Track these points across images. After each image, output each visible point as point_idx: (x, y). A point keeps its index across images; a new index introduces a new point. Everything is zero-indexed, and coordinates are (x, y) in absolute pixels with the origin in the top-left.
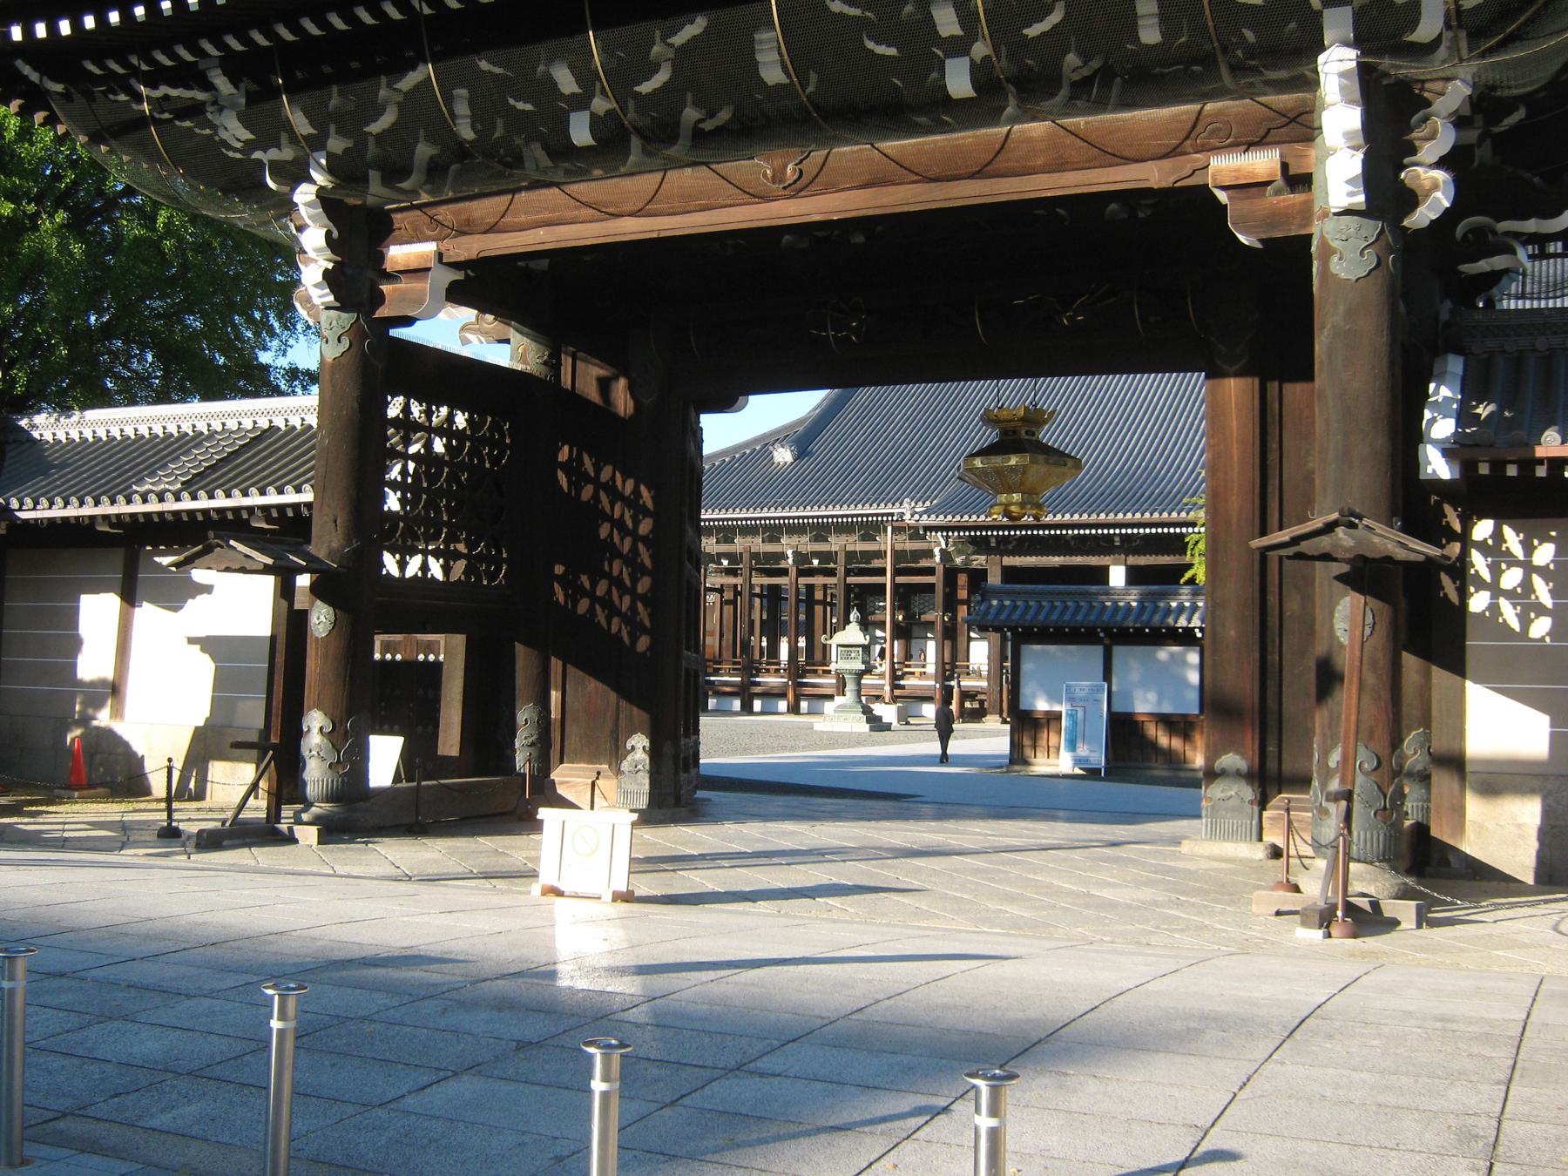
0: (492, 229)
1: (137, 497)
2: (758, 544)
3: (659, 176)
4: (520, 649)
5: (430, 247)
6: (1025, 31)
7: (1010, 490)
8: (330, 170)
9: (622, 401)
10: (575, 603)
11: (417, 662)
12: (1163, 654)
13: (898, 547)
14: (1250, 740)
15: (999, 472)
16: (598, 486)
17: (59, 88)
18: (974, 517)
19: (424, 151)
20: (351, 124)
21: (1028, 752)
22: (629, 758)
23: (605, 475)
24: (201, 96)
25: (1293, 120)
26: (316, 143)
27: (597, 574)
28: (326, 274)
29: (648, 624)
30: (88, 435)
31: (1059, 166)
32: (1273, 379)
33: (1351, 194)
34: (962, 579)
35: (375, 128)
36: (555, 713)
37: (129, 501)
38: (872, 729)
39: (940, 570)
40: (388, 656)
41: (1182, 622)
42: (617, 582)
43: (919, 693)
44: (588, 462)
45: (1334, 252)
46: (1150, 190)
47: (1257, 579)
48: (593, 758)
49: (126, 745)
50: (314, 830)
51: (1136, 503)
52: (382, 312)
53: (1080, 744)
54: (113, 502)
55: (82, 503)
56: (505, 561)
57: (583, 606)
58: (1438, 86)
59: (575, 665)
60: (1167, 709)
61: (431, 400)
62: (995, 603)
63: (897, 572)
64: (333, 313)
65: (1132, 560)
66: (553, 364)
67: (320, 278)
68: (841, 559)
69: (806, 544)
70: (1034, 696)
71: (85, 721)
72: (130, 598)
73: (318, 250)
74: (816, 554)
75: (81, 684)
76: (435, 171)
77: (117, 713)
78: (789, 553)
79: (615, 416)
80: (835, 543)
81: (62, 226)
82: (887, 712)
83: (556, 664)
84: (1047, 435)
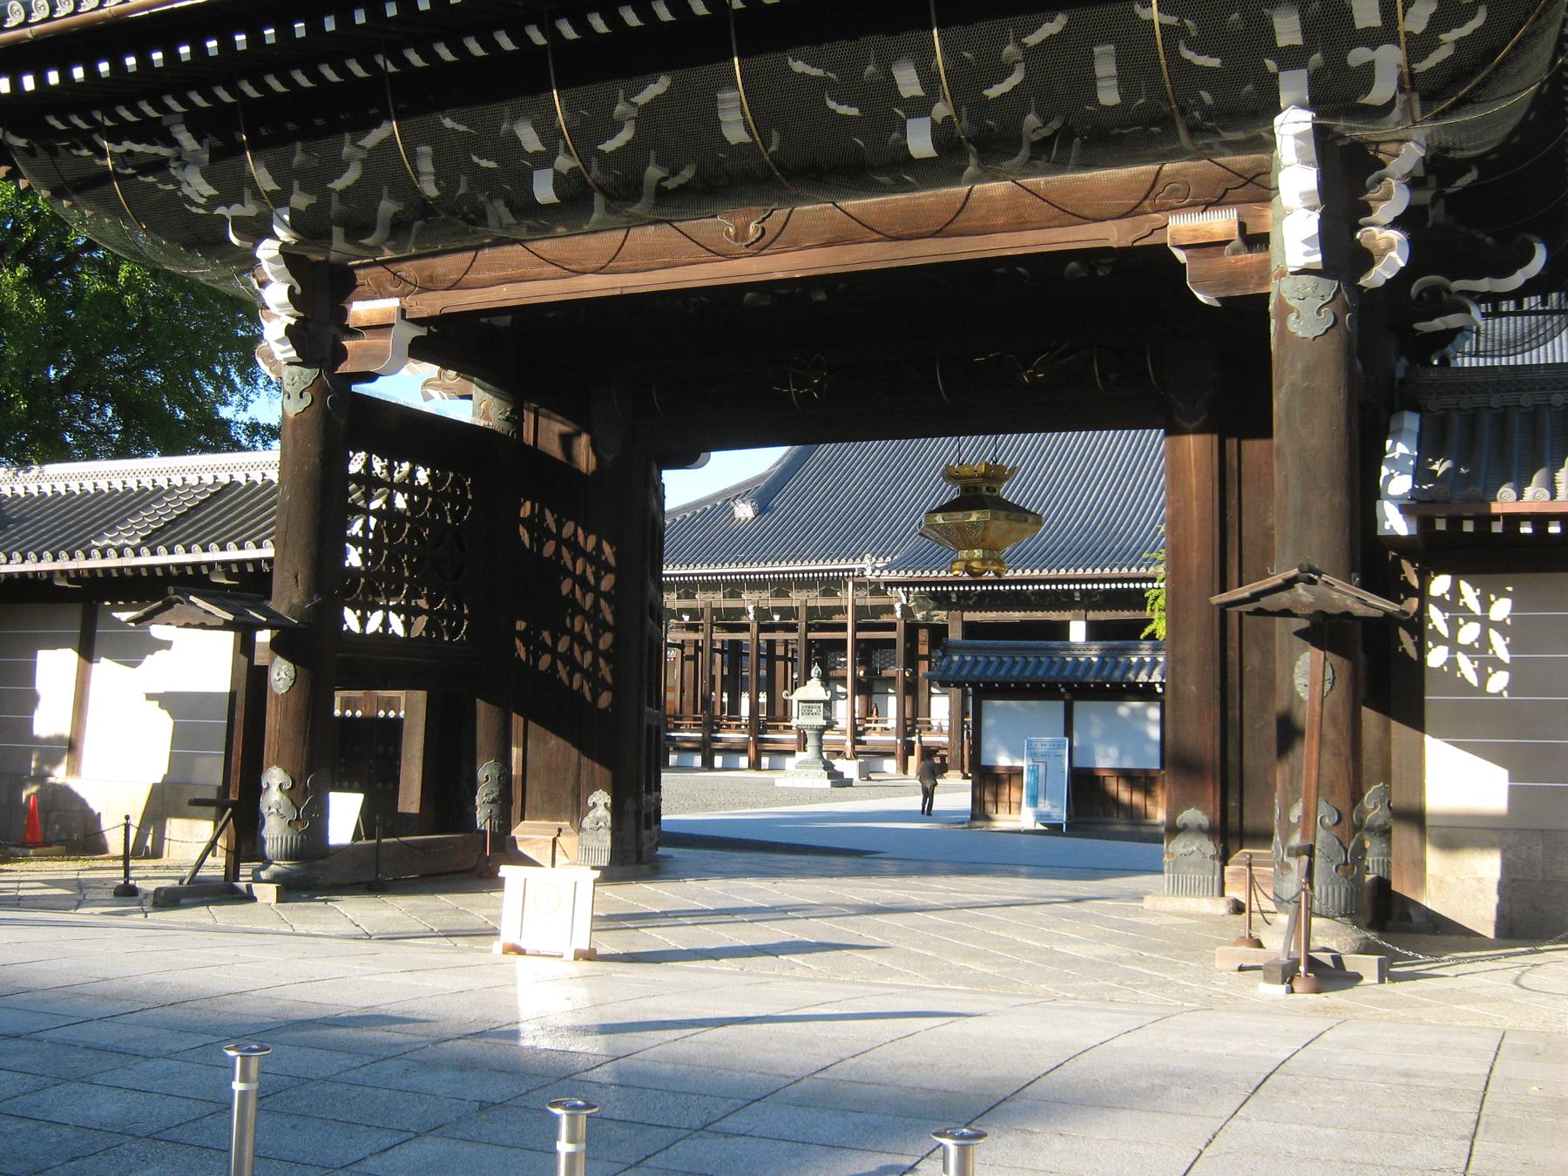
0: (455, 285)
1: (95, 552)
2: (719, 600)
3: (622, 233)
4: (481, 706)
5: (393, 304)
6: (986, 92)
7: (971, 547)
8: (293, 226)
9: (584, 457)
10: (537, 659)
11: (377, 719)
12: (1124, 709)
13: (859, 602)
14: (1211, 794)
15: (960, 528)
16: (560, 541)
17: (22, 143)
18: (935, 573)
19: (387, 208)
20: (315, 181)
21: (990, 808)
22: (591, 815)
23: (568, 530)
24: (164, 152)
25: (1250, 181)
26: (280, 199)
27: (559, 631)
28: (289, 330)
29: (609, 679)
30: (47, 490)
31: (1020, 225)
32: (1231, 436)
33: (1307, 254)
34: (923, 635)
35: (339, 184)
36: (516, 770)
37: (88, 556)
38: (833, 785)
39: (901, 625)
40: (349, 713)
41: (1143, 678)
42: (579, 638)
43: (880, 749)
44: (550, 519)
45: (1291, 310)
46: (1109, 249)
47: (1217, 633)
48: (553, 815)
49: (83, 802)
50: (272, 888)
51: (1096, 561)
52: (345, 368)
53: (1041, 800)
54: (72, 557)
55: (40, 558)
56: (466, 617)
57: (545, 662)
58: (1392, 148)
59: (536, 721)
60: (1128, 764)
61: (392, 454)
62: (956, 658)
63: (858, 627)
64: (296, 369)
65: (1092, 615)
66: (515, 420)
67: (283, 334)
68: (802, 615)
69: (767, 599)
70: (995, 752)
71: (41, 777)
72: (87, 653)
73: (280, 306)
74: (777, 610)
75: (37, 740)
76: (398, 228)
77: (74, 769)
78: (750, 608)
79: (578, 471)
80: (796, 599)
81: (23, 280)
82: (848, 768)
83: (517, 721)
84: (1008, 492)
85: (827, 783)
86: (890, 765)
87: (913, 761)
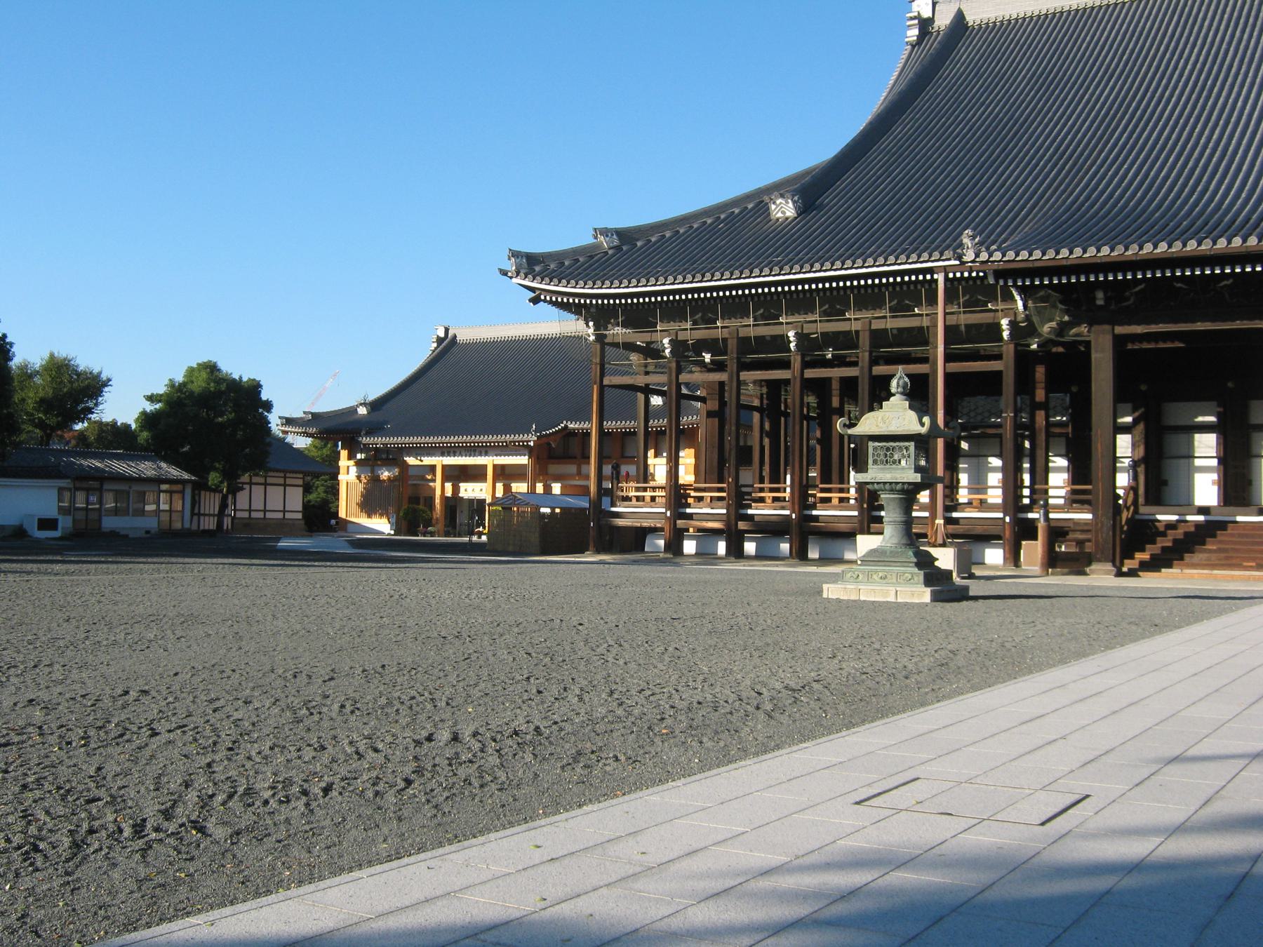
13: (952, 320)
18: (1078, 252)
34: (1040, 372)
38: (936, 598)
39: (1009, 351)
43: (979, 530)
63: (949, 358)
68: (865, 341)
69: (817, 324)
78: (791, 334)
80: (855, 320)
85: (924, 595)
86: (994, 556)
87: (1033, 551)
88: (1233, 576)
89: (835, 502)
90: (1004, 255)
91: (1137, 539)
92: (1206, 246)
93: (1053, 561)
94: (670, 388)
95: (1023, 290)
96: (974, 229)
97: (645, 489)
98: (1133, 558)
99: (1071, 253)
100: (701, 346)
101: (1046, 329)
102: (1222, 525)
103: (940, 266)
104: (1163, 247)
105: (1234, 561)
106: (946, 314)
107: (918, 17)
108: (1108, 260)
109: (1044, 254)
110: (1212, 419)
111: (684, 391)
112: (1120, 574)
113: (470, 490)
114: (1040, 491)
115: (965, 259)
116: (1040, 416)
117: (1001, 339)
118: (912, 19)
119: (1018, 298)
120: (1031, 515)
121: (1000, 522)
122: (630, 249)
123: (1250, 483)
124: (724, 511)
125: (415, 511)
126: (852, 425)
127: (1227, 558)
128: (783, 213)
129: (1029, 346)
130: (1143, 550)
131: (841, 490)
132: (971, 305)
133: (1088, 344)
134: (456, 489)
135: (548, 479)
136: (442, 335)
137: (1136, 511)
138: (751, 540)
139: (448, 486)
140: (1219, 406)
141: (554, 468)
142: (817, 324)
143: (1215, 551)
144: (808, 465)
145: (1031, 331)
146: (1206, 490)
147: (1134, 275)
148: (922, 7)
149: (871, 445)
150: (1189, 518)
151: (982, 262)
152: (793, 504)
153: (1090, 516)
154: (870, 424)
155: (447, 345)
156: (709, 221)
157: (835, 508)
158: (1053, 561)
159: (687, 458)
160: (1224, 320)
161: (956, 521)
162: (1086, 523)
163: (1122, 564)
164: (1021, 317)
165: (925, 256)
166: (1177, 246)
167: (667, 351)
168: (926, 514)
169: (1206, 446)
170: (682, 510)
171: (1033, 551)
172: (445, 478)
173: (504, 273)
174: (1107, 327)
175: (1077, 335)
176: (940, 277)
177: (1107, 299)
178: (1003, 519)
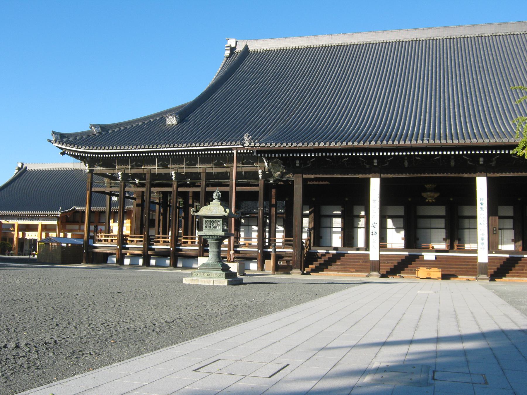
2: (155, 169)
13: (239, 170)
18: (290, 144)
34: (274, 192)
38: (230, 283)
39: (261, 183)
43: (248, 256)
63: (237, 185)
65: (382, 176)
68: (203, 177)
69: (184, 169)
78: (173, 173)
80: (200, 168)
85: (225, 282)
86: (254, 266)
87: (269, 264)
88: (346, 275)
89: (189, 243)
90: (260, 144)
91: (310, 260)
92: (339, 144)
93: (277, 268)
94: (120, 194)
95: (268, 159)
96: (249, 133)
97: (108, 236)
98: (308, 268)
99: (287, 145)
100: (135, 176)
101: (276, 175)
102: (343, 255)
103: (235, 147)
104: (322, 144)
105: (347, 269)
106: (237, 167)
107: (230, 46)
108: (301, 148)
109: (276, 145)
110: (339, 212)
111: (127, 195)
112: (303, 274)
113: (30, 235)
114: (272, 240)
115: (245, 145)
116: (273, 210)
117: (259, 178)
118: (227, 47)
119: (265, 162)
120: (269, 250)
121: (257, 253)
122: (106, 133)
123: (353, 238)
124: (142, 246)
125: (4, 244)
126: (197, 211)
127: (344, 268)
128: (171, 122)
129: (269, 181)
130: (312, 264)
131: (192, 238)
132: (247, 164)
133: (293, 181)
134: (24, 235)
135: (65, 231)
136: (20, 166)
137: (310, 249)
138: (154, 259)
139: (20, 234)
140: (342, 207)
141: (69, 227)
142: (184, 169)
143: (340, 265)
144: (178, 228)
145: (270, 175)
146: (337, 241)
147: (311, 155)
148: (232, 42)
149: (204, 219)
150: (330, 252)
151: (252, 147)
152: (172, 244)
153: (292, 250)
154: (204, 211)
155: (23, 172)
156: (140, 124)
157: (189, 246)
158: (277, 268)
159: (127, 223)
160: (344, 174)
161: (239, 252)
162: (290, 253)
163: (304, 270)
164: (267, 169)
165: (229, 143)
166: (328, 144)
167: (120, 178)
168: (227, 249)
169: (337, 223)
170: (124, 246)
171: (269, 264)
172: (19, 230)
173: (50, 141)
174: (300, 175)
175: (288, 178)
176: (235, 152)
177: (300, 164)
178: (258, 251)
